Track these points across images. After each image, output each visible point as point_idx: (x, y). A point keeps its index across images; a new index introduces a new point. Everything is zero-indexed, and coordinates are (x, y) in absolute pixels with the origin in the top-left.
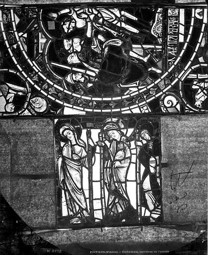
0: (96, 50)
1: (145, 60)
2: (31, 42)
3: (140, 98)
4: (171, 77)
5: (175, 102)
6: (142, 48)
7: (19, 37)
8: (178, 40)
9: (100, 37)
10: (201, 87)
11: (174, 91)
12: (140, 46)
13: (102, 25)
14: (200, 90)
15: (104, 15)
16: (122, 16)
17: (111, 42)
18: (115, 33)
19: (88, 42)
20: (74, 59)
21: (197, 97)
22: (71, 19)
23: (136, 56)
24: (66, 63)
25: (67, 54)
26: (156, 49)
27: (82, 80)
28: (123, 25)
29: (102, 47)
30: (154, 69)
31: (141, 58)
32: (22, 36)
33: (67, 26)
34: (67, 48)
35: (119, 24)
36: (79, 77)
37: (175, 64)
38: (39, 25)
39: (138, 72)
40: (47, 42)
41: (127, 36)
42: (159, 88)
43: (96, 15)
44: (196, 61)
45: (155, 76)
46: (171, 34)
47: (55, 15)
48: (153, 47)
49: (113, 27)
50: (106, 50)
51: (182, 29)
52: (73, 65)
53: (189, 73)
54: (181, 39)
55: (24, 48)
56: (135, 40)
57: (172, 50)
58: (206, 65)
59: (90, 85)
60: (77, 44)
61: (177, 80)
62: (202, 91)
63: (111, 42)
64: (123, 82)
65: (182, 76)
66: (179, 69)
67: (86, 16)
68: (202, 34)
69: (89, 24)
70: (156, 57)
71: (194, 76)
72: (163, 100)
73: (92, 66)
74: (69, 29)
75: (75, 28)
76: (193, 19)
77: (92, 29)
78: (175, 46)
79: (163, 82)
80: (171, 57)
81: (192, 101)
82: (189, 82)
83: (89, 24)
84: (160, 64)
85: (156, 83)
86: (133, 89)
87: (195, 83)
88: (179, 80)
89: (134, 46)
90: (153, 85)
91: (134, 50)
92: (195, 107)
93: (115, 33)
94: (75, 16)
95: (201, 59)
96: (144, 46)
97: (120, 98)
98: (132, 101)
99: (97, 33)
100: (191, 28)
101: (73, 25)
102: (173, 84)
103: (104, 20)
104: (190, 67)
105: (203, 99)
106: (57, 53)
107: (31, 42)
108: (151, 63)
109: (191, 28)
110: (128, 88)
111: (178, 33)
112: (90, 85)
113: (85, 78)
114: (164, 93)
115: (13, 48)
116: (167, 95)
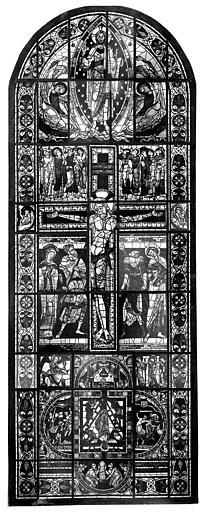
19: (62, 419)
20: (57, 415)
106: (59, 410)
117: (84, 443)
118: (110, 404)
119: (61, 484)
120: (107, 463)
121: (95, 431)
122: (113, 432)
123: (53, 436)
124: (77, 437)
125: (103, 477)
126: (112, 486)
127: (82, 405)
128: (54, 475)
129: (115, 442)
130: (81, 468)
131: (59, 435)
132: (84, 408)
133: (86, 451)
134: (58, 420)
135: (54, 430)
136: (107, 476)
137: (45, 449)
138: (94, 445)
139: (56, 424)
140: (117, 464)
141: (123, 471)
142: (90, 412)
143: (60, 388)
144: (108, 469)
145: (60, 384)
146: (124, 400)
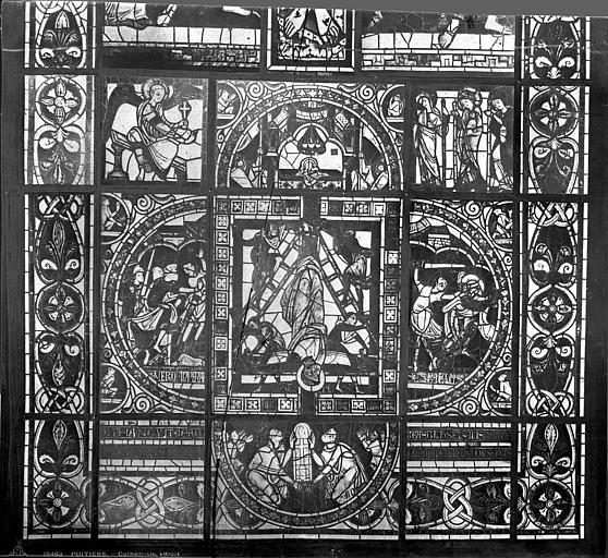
1: (156, 347)
9: (179, 302)
13: (192, 304)
19: (174, 287)
20: (158, 273)
22: (197, 271)
36: (139, 279)
40: (175, 246)
41: (180, 329)
45: (141, 357)
47: (201, 256)
51: (187, 386)
52: (151, 273)
94: (200, 276)
99: (183, 298)
106: (164, 256)
108: (154, 354)
117: (244, 363)
118: (329, 239)
119: (170, 492)
120: (319, 427)
121: (282, 326)
122: (338, 329)
123: (146, 339)
124: (222, 343)
125: (303, 473)
126: (335, 504)
127: (240, 243)
128: (150, 464)
129: (343, 360)
130: (236, 441)
131: (165, 339)
132: (247, 251)
133: (250, 388)
134: (160, 288)
135: (148, 321)
136: (316, 469)
137: (120, 382)
138: (277, 370)
139: (155, 300)
140: (349, 432)
141: (366, 456)
142: (265, 260)
143: (171, 188)
144: (320, 447)
145: (171, 173)
146: (373, 227)
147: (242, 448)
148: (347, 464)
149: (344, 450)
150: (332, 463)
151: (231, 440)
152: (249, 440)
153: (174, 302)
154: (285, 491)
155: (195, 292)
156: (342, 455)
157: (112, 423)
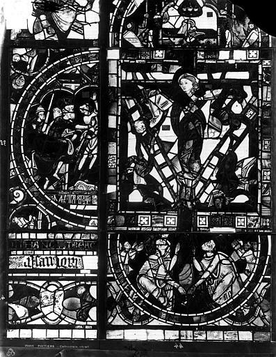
0: (64, 132)
1: (55, 175)
2: (72, 77)
3: (23, 169)
4: (40, 197)
5: (19, 200)
6: (66, 173)
7: (76, 67)
8: (72, 204)
9: (75, 136)
10: (30, 222)
11: (28, 199)
12: (67, 171)
13: (85, 138)
14: (27, 222)
15: (94, 140)
16: (93, 155)
17: (71, 146)
18: (78, 149)
19: (71, 125)
21: (22, 219)
22: (91, 111)
23: (59, 167)
24: (53, 106)
25: (62, 107)
26: (65, 185)
27: (39, 120)
28: (85, 156)
29: (67, 137)
30: (47, 182)
31: (57, 172)
32: (77, 69)
33: (86, 108)
34: (66, 107)
35: (86, 152)
37: (52, 201)
38: (86, 84)
39: (45, 171)
40: (72, 90)
42: (31, 186)
43: (94, 133)
44: (53, 219)
45: (41, 183)
46: (76, 198)
47: (94, 98)
48: (67, 182)
49: (83, 149)
50: (65, 141)
51: (81, 207)
52: (52, 113)
53: (43, 214)
54: (73, 207)
55: (68, 71)
56: (73, 166)
57: (63, 198)
58: (49, 228)
59: (34, 127)
60: (70, 116)
61: (38, 202)
62: (27, 224)
63: (71, 146)
64: (37, 156)
65: (41, 207)
66: (48, 205)
67: (93, 124)
68: (76, 225)
69: (86, 127)
70: (58, 185)
71: (40, 216)
72: (19, 189)
73: (50, 129)
74: (83, 109)
75: (84, 115)
76: (89, 217)
77: (82, 130)
78: (67, 201)
79: (36, 190)
80: (58, 198)
81: (18, 215)
82: (35, 212)
83: (86, 127)
84: (51, 188)
85: (35, 184)
86: (30, 164)
87: (34, 218)
88: (38, 205)
89: (67, 165)
90: (34, 181)
91: (64, 166)
92: (13, 217)
93: (78, 149)
94: (93, 115)
95: (54, 224)
96: (67, 174)
97: (22, 152)
98: (20, 162)
99: (79, 134)
100: (82, 216)
101: (86, 113)
102: (34, 198)
103: (89, 139)
104: (48, 214)
105: (20, 224)
106: (62, 99)
107: (72, 77)
108: (52, 180)
109: (82, 216)
110: (31, 159)
111: (77, 204)
112: (34, 127)
113: (41, 123)
114: (26, 190)
115: (67, 62)
116: (24, 193)
147: (133, 255)
148: (224, 269)
149: (222, 257)
150: (210, 269)
151: (123, 249)
152: (139, 250)
153: (70, 137)
154: (170, 294)
155: (89, 128)
156: (220, 262)
157: (19, 236)
